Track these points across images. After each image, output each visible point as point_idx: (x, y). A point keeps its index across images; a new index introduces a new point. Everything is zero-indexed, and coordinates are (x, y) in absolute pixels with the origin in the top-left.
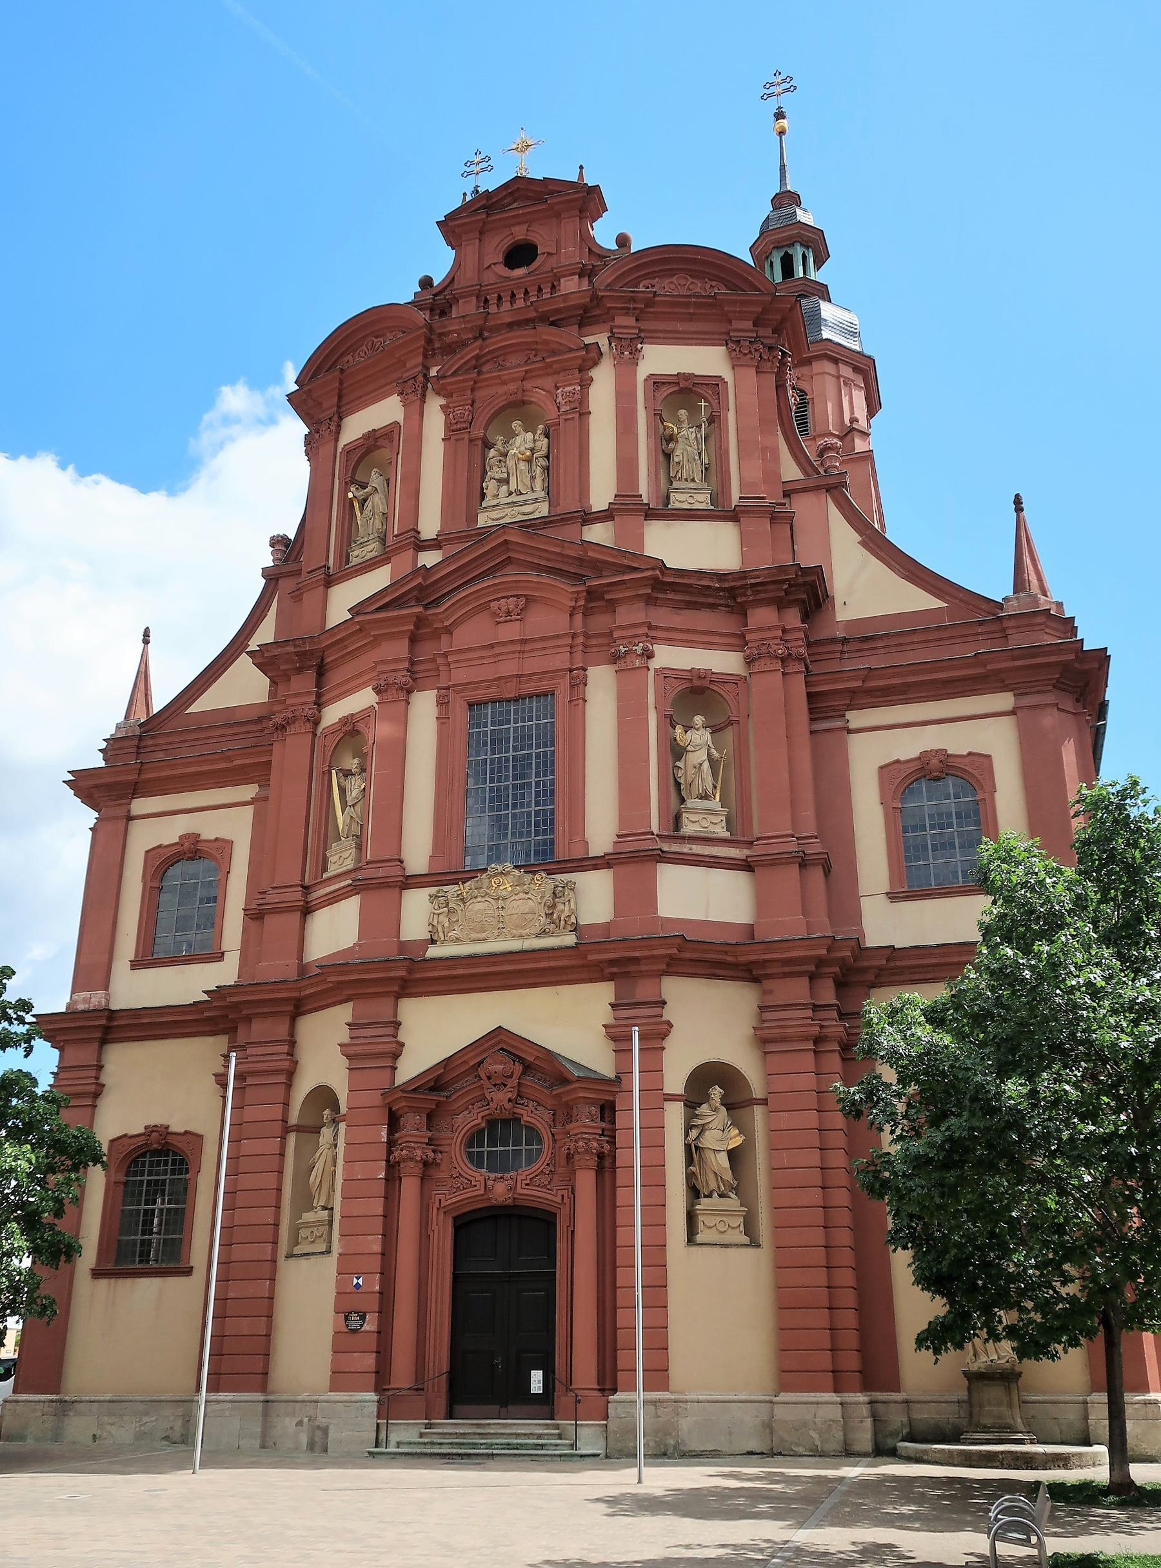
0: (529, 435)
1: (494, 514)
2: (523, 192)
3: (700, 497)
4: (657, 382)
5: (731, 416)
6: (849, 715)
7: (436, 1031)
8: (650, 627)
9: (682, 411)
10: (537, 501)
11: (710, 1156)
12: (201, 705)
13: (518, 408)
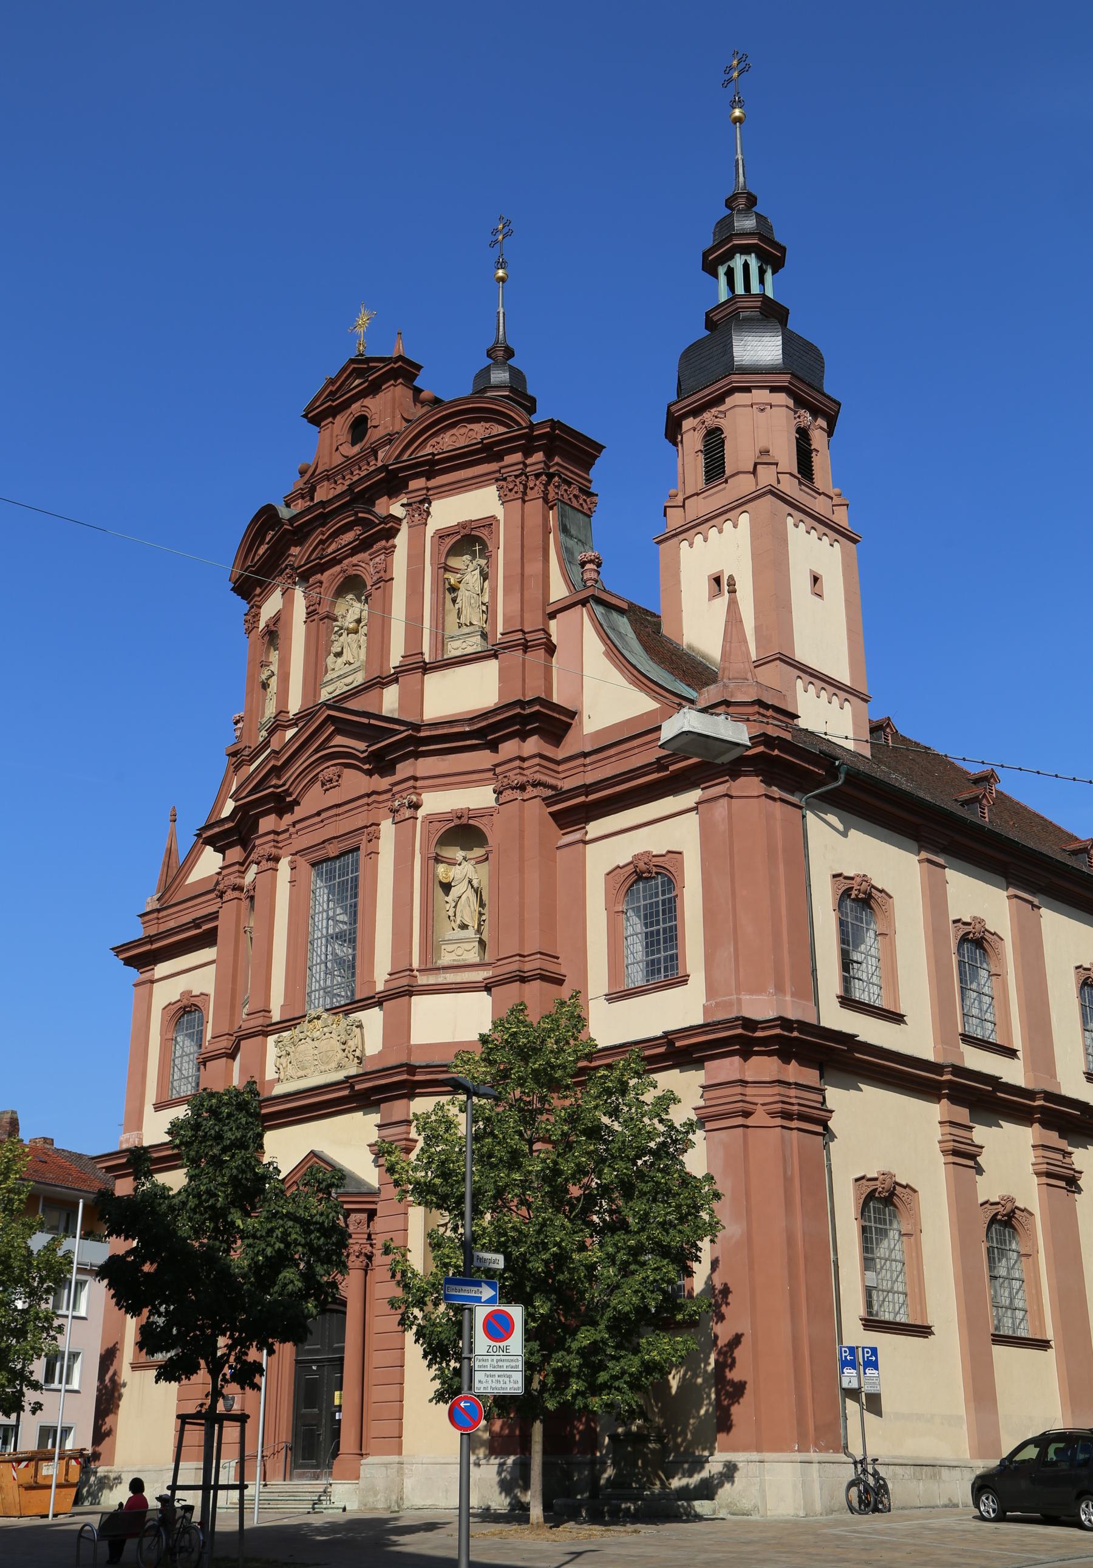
1: (330, 688)
8: (416, 779)
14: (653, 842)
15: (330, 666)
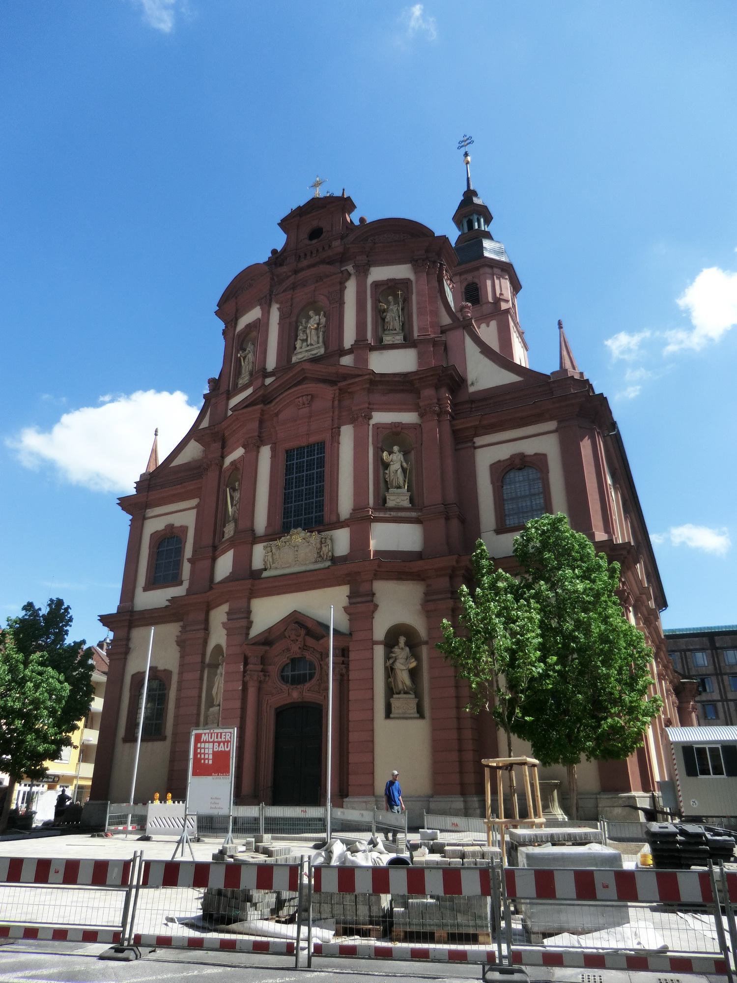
0: (317, 317)
1: (300, 356)
2: (316, 205)
3: (398, 337)
4: (376, 285)
5: (414, 297)
6: (476, 439)
7: (268, 612)
9: (390, 298)
10: (319, 347)
11: (399, 673)
12: (175, 463)
13: (313, 305)
14: (529, 447)
15: (298, 346)
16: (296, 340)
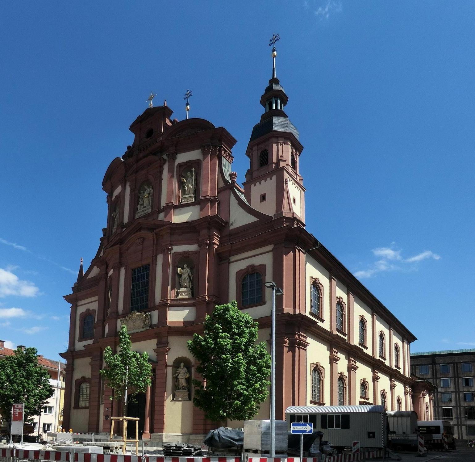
1: (139, 215)
13: (147, 182)
16: (138, 204)
